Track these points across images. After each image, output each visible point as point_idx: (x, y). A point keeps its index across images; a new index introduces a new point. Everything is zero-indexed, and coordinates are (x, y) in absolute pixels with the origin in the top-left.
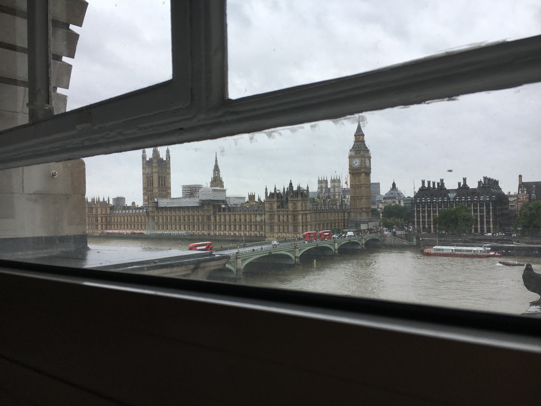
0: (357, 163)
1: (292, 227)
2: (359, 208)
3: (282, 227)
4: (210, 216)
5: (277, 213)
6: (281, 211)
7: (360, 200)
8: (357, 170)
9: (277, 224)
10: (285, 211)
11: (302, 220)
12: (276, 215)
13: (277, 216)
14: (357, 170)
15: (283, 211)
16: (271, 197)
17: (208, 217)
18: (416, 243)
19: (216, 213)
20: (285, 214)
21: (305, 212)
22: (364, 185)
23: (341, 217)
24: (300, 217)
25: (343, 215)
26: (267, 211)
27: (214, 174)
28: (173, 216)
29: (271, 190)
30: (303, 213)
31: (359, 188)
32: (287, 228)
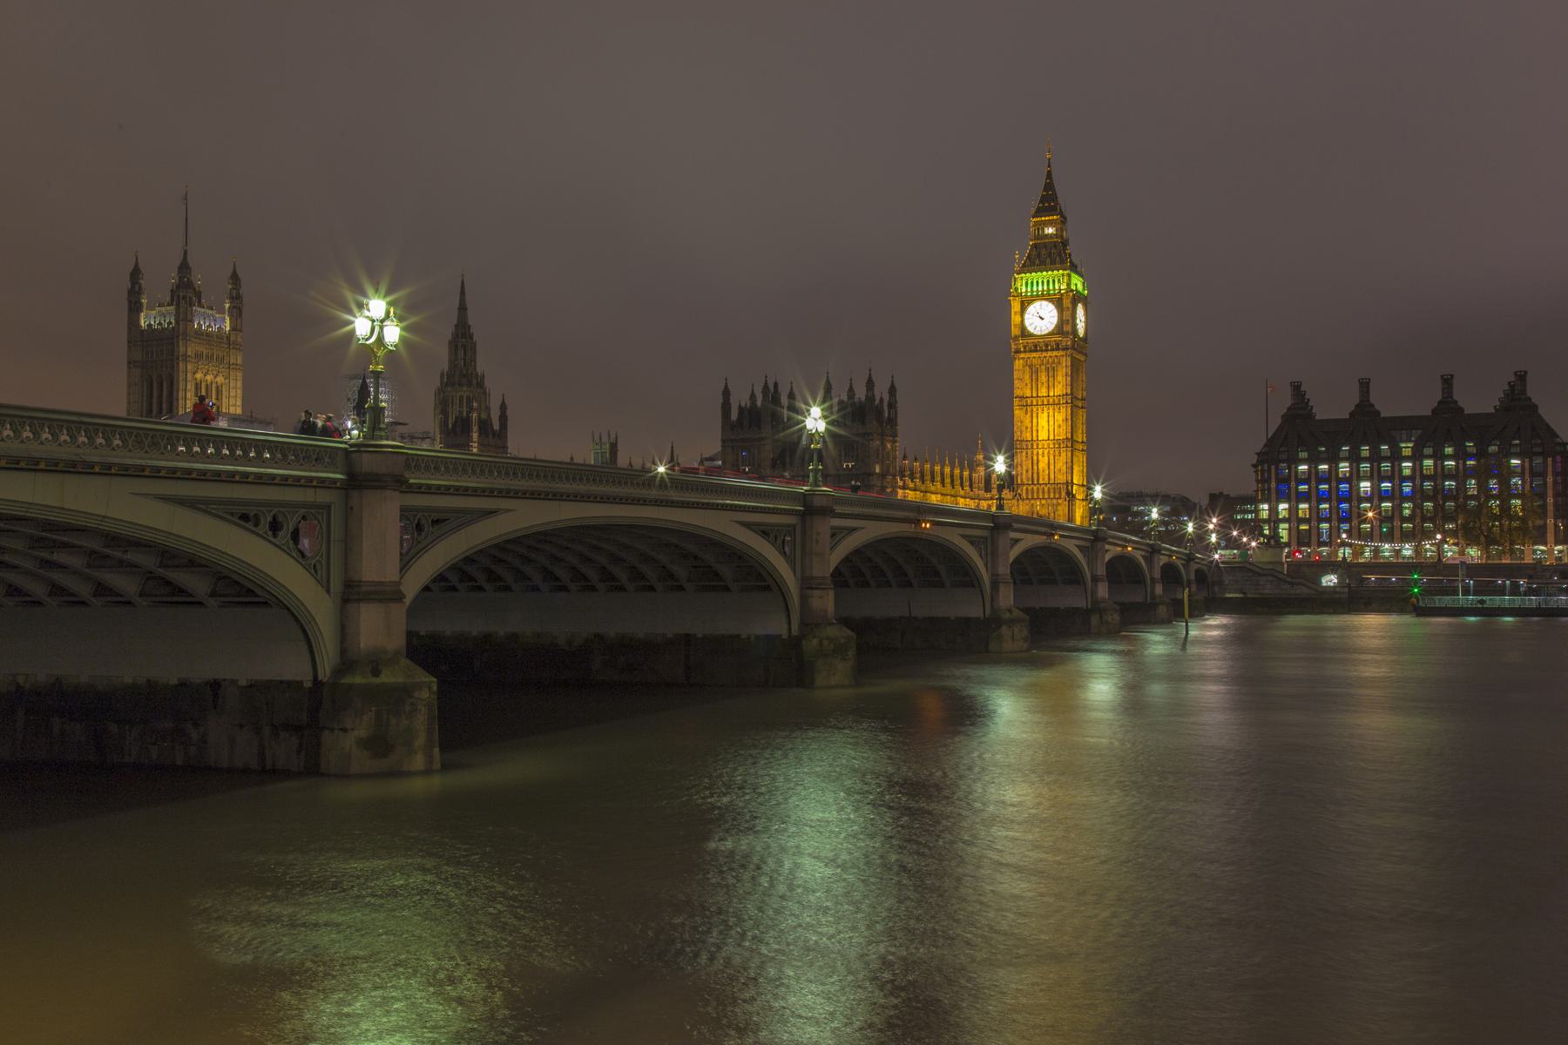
18: (1346, 590)
29: (740, 398)
31: (1051, 414)
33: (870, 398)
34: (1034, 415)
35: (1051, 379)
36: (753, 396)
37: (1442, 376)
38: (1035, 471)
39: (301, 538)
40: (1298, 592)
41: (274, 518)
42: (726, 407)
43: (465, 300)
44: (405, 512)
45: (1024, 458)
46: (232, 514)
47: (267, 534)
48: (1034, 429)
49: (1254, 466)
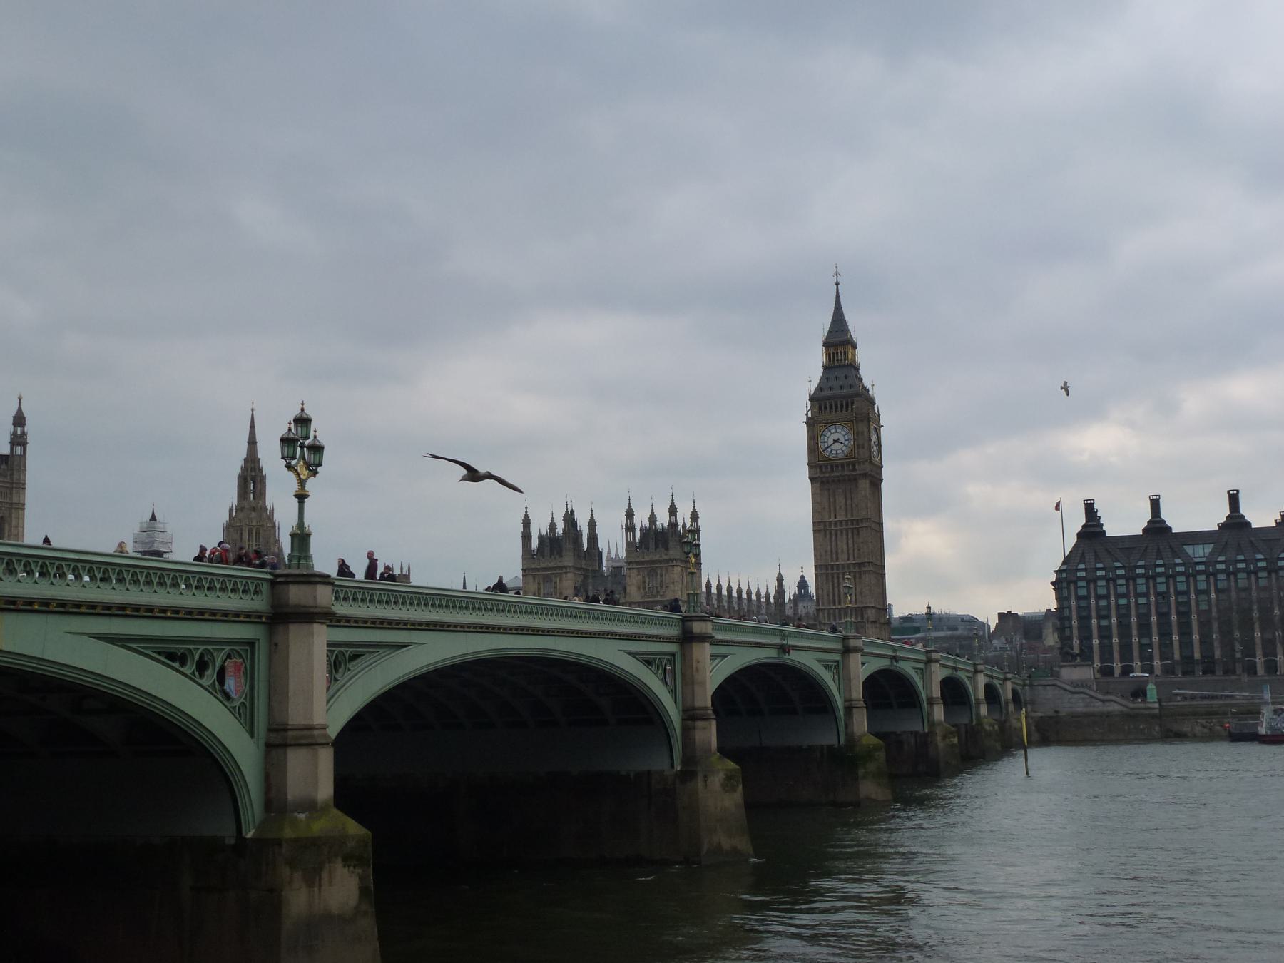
0: (838, 440)
8: (843, 466)
14: (840, 468)
16: (547, 550)
18: (1157, 705)
22: (868, 524)
29: (539, 527)
31: (850, 535)
33: (673, 524)
34: (834, 538)
35: (849, 502)
36: (553, 527)
37: (1229, 492)
39: (227, 678)
40: (1110, 709)
41: (202, 655)
42: (526, 536)
43: (254, 434)
44: (330, 645)
46: (159, 653)
47: (194, 675)
48: (834, 551)
49: (1052, 583)
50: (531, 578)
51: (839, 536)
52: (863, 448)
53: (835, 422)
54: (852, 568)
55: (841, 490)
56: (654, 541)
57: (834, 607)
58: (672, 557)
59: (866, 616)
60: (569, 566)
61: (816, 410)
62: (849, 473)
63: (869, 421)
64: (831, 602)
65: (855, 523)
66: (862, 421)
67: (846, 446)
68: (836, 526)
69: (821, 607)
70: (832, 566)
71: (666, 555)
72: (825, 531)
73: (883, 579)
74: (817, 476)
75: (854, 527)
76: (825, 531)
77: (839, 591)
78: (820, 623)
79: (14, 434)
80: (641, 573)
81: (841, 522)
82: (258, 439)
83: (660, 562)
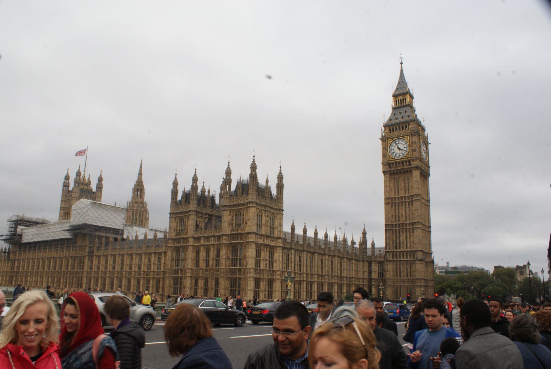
1: (228, 282)
2: (407, 252)
3: (203, 281)
4: (84, 257)
5: (195, 243)
6: (202, 239)
7: (408, 233)
8: (403, 163)
9: (192, 273)
10: (214, 236)
11: (258, 263)
12: (190, 249)
13: (192, 251)
14: (401, 164)
15: (208, 238)
17: (81, 260)
19: (93, 252)
20: (213, 245)
21: (267, 241)
23: (363, 272)
24: (251, 252)
25: (366, 269)
26: (172, 239)
27: (134, 196)
28: (36, 261)
30: (260, 241)
31: (407, 206)
32: (213, 286)
34: (397, 207)
38: (398, 242)
42: (175, 192)
45: (391, 235)
48: (397, 216)
50: (174, 219)
51: (400, 206)
52: (415, 151)
53: (398, 137)
54: (408, 226)
55: (402, 178)
56: (241, 190)
57: (396, 251)
58: (249, 200)
59: (416, 256)
60: (192, 211)
61: (387, 131)
62: (407, 167)
63: (419, 136)
64: (395, 247)
65: (410, 197)
66: (415, 135)
67: (405, 151)
68: (398, 200)
69: (388, 250)
70: (396, 224)
71: (247, 199)
72: (392, 203)
73: (429, 235)
74: (387, 170)
75: (410, 200)
76: (392, 203)
77: (400, 240)
78: (387, 260)
79: (98, 185)
80: (231, 214)
81: (402, 197)
82: (143, 173)
83: (243, 205)
